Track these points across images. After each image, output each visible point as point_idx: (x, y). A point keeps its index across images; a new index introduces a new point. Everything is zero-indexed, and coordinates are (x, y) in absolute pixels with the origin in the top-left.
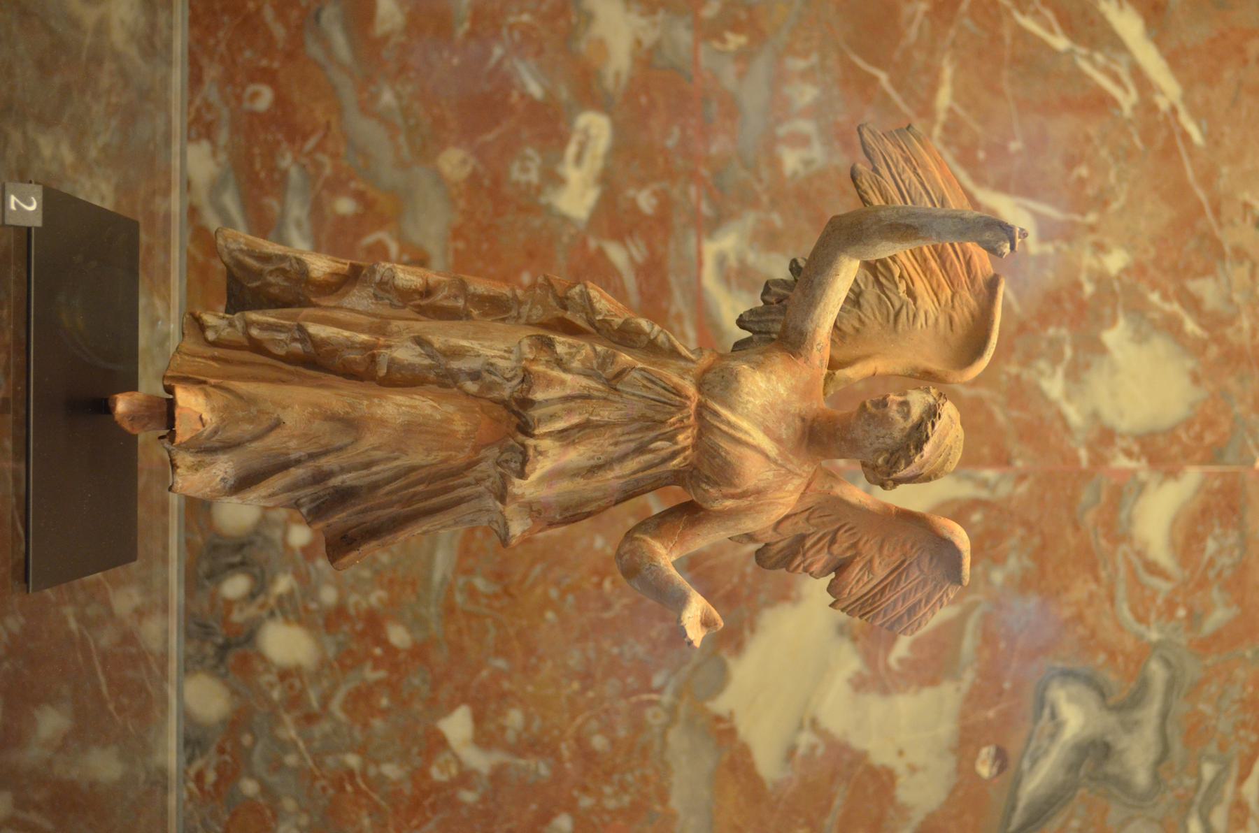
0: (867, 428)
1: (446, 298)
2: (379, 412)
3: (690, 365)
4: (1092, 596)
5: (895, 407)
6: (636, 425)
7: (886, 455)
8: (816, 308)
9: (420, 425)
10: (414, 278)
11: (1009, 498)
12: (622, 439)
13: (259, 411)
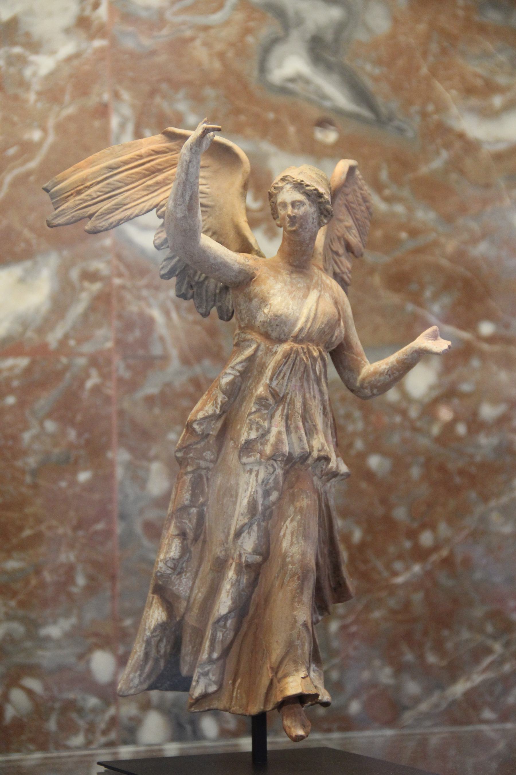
0: (307, 230)
1: (190, 521)
2: (298, 557)
3: (262, 347)
4: (205, 44)
5: (296, 211)
6: (305, 384)
7: (323, 217)
8: (227, 262)
9: (305, 529)
10: (174, 545)
11: (133, 106)
12: (312, 394)
13: (298, 639)
